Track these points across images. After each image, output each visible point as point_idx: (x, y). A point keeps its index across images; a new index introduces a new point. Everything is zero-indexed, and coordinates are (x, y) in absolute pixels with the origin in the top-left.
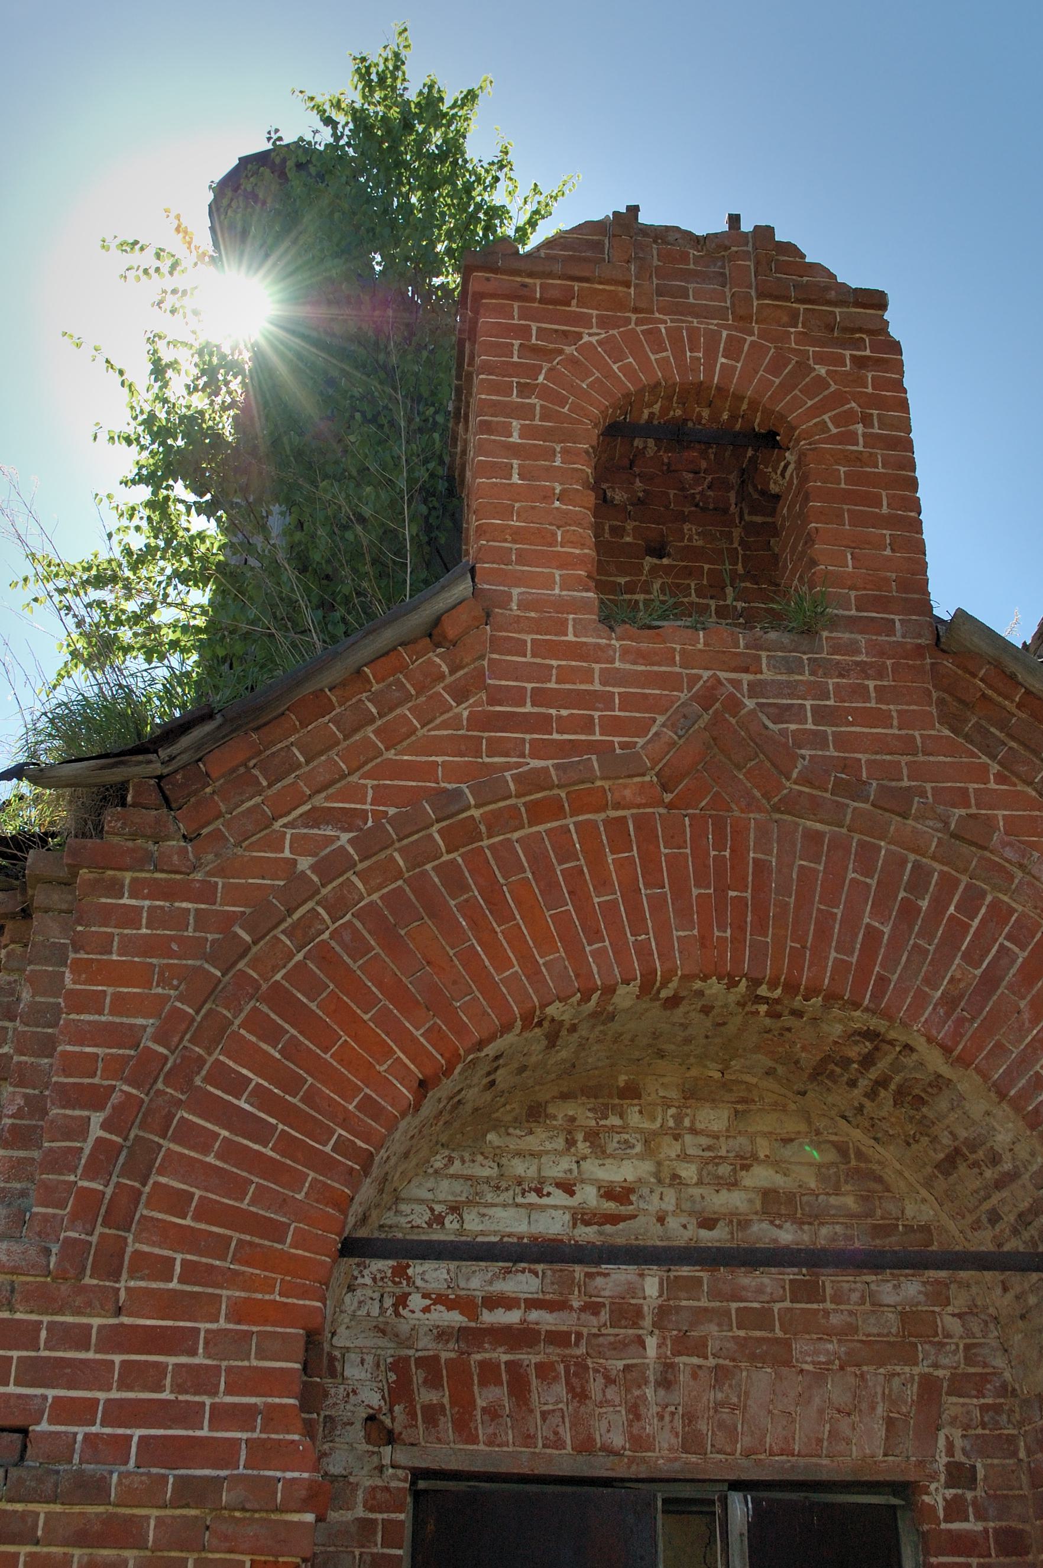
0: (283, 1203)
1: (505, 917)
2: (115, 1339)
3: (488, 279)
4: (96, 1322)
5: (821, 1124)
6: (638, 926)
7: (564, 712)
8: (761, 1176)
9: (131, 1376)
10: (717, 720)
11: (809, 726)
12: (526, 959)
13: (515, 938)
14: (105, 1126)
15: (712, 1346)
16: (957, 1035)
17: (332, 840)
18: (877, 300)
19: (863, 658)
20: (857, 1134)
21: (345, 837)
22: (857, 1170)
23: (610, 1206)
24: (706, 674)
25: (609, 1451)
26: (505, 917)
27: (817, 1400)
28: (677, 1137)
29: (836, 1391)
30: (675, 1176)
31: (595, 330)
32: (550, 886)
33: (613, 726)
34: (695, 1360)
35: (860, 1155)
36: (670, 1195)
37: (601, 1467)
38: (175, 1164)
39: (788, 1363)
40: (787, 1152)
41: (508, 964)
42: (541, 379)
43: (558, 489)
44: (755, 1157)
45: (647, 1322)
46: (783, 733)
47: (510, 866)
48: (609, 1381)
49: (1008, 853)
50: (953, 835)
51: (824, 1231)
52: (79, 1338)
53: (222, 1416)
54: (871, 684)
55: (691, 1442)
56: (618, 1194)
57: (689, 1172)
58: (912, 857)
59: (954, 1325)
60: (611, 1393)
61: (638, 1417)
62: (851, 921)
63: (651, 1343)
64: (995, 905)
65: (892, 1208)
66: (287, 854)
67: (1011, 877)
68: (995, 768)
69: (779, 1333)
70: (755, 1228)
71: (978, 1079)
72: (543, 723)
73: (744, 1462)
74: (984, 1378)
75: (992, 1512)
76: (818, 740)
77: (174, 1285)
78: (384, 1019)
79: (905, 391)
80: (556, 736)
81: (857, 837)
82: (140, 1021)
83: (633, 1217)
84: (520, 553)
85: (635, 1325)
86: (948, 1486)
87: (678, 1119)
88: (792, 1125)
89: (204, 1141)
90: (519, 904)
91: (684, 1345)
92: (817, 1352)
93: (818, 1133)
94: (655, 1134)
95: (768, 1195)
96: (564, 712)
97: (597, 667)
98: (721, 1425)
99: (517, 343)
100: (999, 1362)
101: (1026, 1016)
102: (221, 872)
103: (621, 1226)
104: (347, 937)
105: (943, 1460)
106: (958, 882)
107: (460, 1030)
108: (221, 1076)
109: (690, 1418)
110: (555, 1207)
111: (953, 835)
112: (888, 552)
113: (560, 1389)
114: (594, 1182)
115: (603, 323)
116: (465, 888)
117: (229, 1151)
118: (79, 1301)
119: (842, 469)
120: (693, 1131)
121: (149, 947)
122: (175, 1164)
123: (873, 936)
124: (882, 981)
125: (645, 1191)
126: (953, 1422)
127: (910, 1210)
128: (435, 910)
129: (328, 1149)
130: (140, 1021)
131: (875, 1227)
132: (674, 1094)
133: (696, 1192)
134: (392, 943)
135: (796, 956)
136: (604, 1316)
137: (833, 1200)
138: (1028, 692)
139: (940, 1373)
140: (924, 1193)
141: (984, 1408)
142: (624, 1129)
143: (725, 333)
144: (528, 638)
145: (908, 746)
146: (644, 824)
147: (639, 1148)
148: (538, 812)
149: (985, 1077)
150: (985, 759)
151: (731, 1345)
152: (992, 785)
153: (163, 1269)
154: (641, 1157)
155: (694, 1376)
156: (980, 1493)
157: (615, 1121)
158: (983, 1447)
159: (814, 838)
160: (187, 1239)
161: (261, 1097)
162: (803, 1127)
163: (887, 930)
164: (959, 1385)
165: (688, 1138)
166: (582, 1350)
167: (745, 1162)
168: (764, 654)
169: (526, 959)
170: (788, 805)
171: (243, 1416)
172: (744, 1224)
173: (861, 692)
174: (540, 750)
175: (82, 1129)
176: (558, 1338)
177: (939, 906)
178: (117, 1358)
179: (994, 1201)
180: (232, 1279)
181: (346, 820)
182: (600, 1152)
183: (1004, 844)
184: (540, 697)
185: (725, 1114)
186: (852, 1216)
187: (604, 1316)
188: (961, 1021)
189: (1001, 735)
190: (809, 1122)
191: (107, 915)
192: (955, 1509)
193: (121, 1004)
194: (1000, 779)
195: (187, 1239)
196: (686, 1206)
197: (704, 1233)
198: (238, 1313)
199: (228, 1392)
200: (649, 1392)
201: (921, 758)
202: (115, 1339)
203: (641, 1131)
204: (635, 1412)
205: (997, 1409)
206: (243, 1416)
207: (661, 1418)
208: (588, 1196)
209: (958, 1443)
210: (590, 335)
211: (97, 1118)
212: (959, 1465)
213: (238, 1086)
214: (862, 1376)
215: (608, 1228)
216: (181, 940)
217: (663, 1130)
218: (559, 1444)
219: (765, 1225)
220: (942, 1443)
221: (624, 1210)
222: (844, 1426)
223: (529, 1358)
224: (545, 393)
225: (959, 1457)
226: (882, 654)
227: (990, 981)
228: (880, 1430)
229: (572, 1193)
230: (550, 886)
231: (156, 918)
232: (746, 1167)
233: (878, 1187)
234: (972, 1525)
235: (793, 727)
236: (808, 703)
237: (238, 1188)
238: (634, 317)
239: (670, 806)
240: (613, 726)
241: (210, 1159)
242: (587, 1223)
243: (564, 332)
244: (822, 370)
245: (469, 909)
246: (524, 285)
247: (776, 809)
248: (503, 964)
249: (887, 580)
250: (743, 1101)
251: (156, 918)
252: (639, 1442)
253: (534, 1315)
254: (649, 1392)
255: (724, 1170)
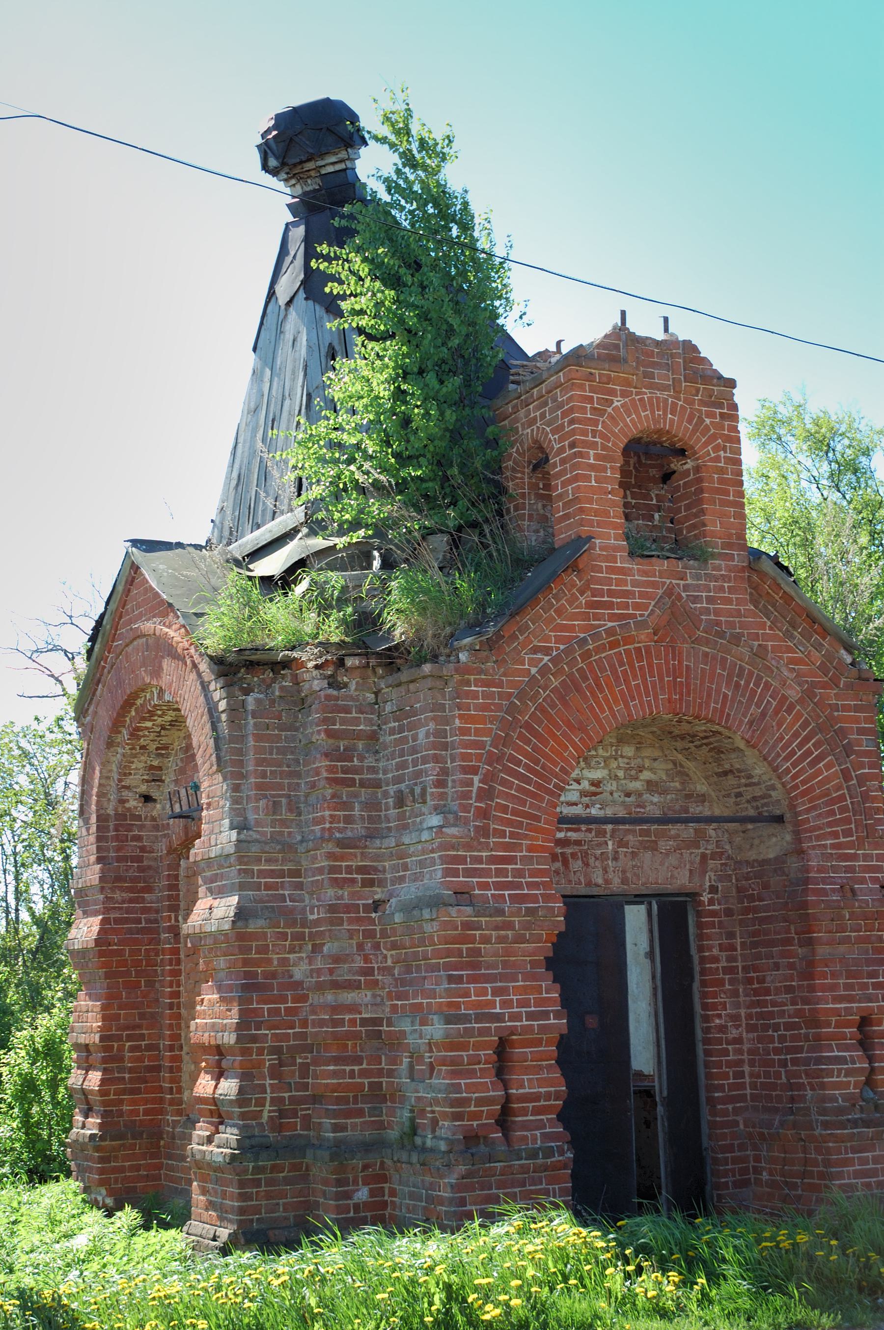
0: (539, 808)
1: (602, 691)
2: (493, 860)
3: (577, 371)
4: (484, 854)
5: (667, 752)
6: (648, 695)
7: (619, 600)
8: (646, 775)
9: (499, 873)
10: (673, 603)
11: (705, 605)
12: (611, 709)
13: (606, 699)
14: (480, 782)
15: (631, 844)
16: (752, 736)
17: (542, 659)
18: (731, 383)
19: (723, 572)
20: (680, 756)
21: (546, 658)
22: (680, 772)
23: (593, 788)
24: (668, 581)
25: (597, 885)
26: (602, 691)
27: (666, 864)
28: (616, 759)
29: (673, 860)
30: (616, 776)
31: (619, 399)
32: (617, 678)
33: (637, 606)
34: (625, 850)
35: (681, 766)
36: (614, 783)
37: (595, 891)
38: (501, 794)
39: (656, 850)
40: (655, 764)
41: (604, 712)
42: (600, 427)
43: (610, 487)
44: (644, 767)
45: (608, 836)
46: (695, 608)
47: (602, 669)
48: (597, 859)
49: (773, 662)
50: (754, 654)
51: (669, 797)
52: (479, 860)
53: (530, 885)
54: (726, 585)
55: (624, 881)
56: (596, 783)
57: (621, 774)
58: (739, 662)
59: (713, 833)
60: (598, 863)
61: (606, 872)
62: (718, 691)
63: (610, 843)
64: (766, 682)
65: (692, 786)
66: (527, 667)
67: (773, 672)
68: (769, 623)
69: (653, 838)
70: (644, 796)
71: (757, 753)
72: (610, 605)
73: (643, 888)
74: (722, 853)
75: (723, 902)
76: (707, 611)
77: (507, 840)
78: (564, 734)
79: (739, 432)
80: (616, 611)
81: (720, 654)
82: (485, 739)
83: (601, 793)
84: (598, 522)
85: (604, 837)
86: (709, 893)
87: (616, 751)
88: (657, 753)
89: (510, 785)
90: (607, 685)
91: (622, 844)
92: (666, 845)
93: (666, 756)
94: (608, 758)
95: (649, 782)
96: (619, 600)
97: (629, 578)
98: (635, 874)
99: (589, 406)
100: (727, 847)
101: (775, 728)
102: (504, 675)
103: (598, 797)
104: (549, 701)
105: (708, 884)
106: (810, 724)
107: (590, 738)
108: (512, 759)
109: (624, 872)
110: (574, 790)
111: (754, 654)
112: (732, 520)
113: (580, 862)
114: (587, 779)
115: (624, 394)
116: (588, 679)
117: (520, 789)
118: (479, 847)
119: (716, 476)
120: (622, 756)
121: (485, 708)
122: (501, 794)
123: (725, 696)
124: (729, 715)
125: (605, 782)
126: (712, 869)
127: (699, 787)
128: (578, 689)
129: (551, 787)
130: (485, 739)
131: (686, 795)
132: (614, 741)
133: (623, 782)
134: (565, 704)
135: (700, 705)
136: (593, 833)
137: (672, 784)
138: (785, 592)
139: (708, 852)
140: (703, 781)
141: (722, 864)
142: (596, 756)
143: (670, 400)
144: (604, 564)
145: (738, 614)
146: (647, 648)
147: (602, 764)
148: (613, 645)
149: (761, 752)
150: (765, 619)
151: (637, 843)
152: (768, 631)
153: (503, 834)
154: (603, 768)
155: (625, 856)
156: (719, 896)
157: (593, 753)
158: (720, 879)
159: (706, 655)
160: (510, 823)
161: (527, 767)
162: (660, 754)
163: (730, 694)
164: (714, 856)
165: (620, 759)
166: (586, 847)
167: (641, 769)
168: (688, 571)
169: (611, 709)
170: (697, 641)
171: (535, 885)
172: (640, 795)
173: (722, 588)
174: (612, 618)
175: (470, 783)
176: (578, 843)
177: (748, 683)
178: (493, 867)
179: (741, 789)
180: (526, 837)
181: (547, 651)
182: (589, 766)
183: (773, 659)
184: (611, 593)
185: (633, 749)
186: (678, 791)
187: (593, 833)
188: (754, 731)
189: (772, 609)
190: (663, 752)
191: (468, 695)
192: (711, 902)
193: (478, 732)
194: (771, 628)
195: (510, 823)
196: (620, 788)
197: (627, 799)
198: (530, 849)
199: (529, 877)
200: (610, 862)
201: (743, 619)
202: (493, 860)
203: (602, 757)
204: (605, 870)
205: (725, 864)
206: (535, 885)
207: (614, 872)
208: (585, 785)
209: (713, 877)
210: (618, 401)
211: (476, 779)
212: (712, 886)
213: (518, 763)
214: (681, 854)
215: (593, 798)
216: (494, 704)
217: (611, 757)
218: (580, 883)
219: (648, 795)
220: (707, 878)
221: (598, 790)
222: (675, 873)
223: (568, 851)
224: (603, 436)
225: (713, 883)
226: (730, 571)
227: (763, 714)
228: (687, 873)
229: (580, 784)
230: (617, 678)
231: (486, 695)
232: (641, 771)
233: (687, 778)
234: (716, 907)
235: (699, 605)
236: (704, 594)
237: (523, 803)
238: (634, 390)
239: (656, 642)
240: (637, 606)
241: (513, 792)
242: (586, 796)
243: (607, 399)
244: (708, 421)
245: (589, 687)
246: (591, 374)
247: (693, 642)
248: (603, 711)
249: (732, 534)
250: (639, 743)
251: (486, 695)
252: (607, 882)
253: (569, 834)
254: (610, 862)
255: (633, 772)
